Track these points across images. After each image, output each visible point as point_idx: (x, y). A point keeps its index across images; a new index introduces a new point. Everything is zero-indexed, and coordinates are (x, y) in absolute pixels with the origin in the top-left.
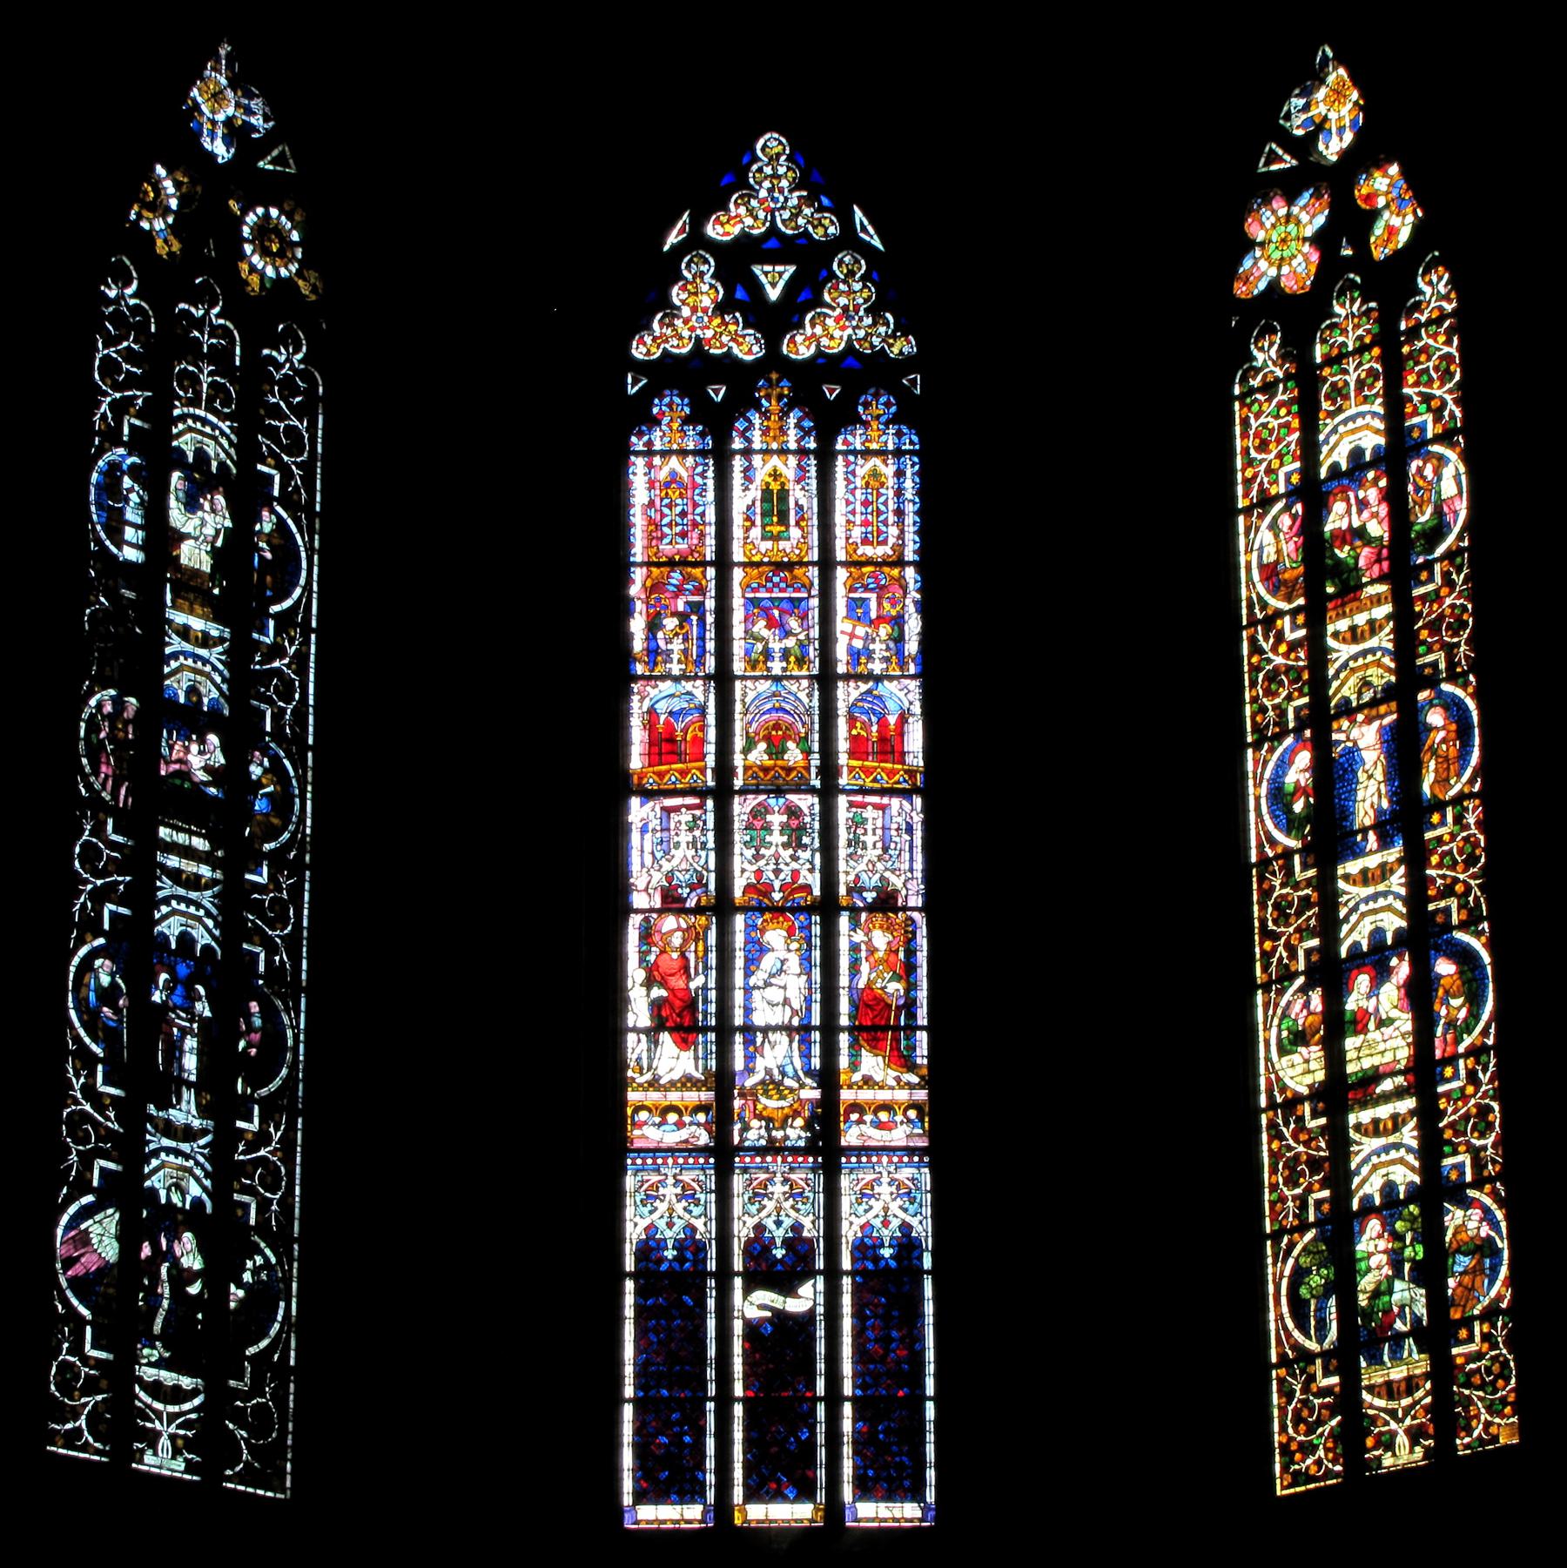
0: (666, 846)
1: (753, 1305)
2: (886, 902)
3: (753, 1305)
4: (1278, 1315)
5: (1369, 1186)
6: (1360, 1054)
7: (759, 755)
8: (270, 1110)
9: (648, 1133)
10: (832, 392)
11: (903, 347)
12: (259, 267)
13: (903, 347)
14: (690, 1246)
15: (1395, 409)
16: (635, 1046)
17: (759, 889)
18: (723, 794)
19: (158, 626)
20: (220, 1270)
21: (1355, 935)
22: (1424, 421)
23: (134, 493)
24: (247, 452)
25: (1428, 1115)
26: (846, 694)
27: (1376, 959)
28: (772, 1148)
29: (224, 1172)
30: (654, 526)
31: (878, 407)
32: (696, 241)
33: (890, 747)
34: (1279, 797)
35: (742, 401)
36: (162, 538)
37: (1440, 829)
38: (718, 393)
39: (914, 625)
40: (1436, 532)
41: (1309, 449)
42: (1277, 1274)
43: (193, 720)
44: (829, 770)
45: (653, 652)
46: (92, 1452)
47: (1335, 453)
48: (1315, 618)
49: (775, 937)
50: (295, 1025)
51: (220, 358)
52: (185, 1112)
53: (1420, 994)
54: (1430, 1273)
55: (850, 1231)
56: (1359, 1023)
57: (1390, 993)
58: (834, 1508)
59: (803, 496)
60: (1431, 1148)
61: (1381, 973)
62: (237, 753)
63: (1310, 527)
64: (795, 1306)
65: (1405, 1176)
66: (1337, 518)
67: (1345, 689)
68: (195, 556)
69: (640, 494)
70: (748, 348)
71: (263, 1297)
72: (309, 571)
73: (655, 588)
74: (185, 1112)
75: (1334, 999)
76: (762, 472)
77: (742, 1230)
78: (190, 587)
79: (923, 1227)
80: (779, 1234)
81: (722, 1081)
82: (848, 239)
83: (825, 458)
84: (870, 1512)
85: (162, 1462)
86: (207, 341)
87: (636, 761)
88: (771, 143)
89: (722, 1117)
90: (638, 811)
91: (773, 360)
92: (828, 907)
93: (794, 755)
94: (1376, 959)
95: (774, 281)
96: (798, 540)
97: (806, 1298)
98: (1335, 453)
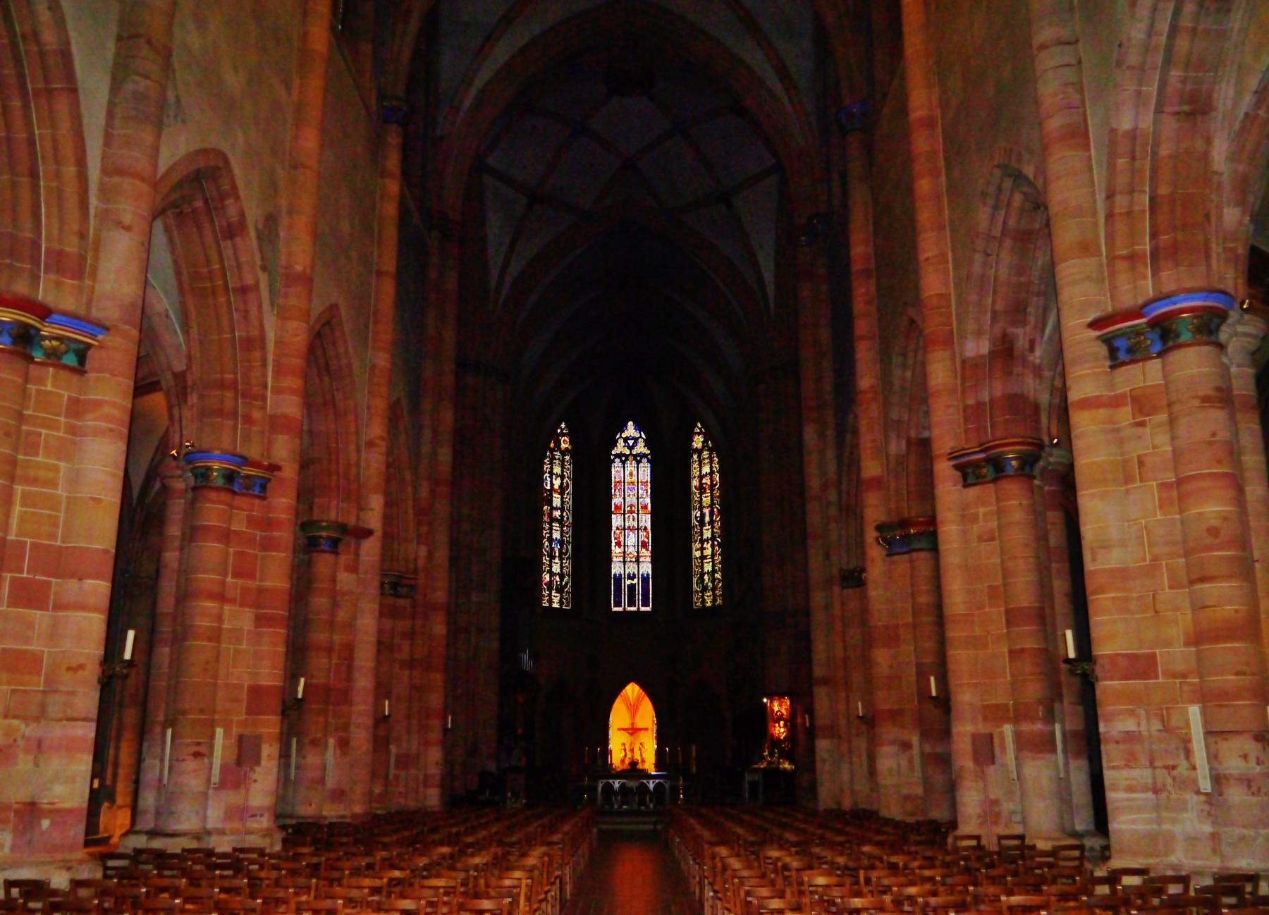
0: (617, 521)
1: (628, 582)
2: (646, 528)
3: (628, 582)
4: (695, 586)
5: (706, 570)
6: (705, 554)
7: (629, 508)
8: (567, 559)
9: (614, 559)
10: (638, 458)
11: (649, 452)
12: (564, 446)
13: (649, 452)
14: (620, 575)
15: (711, 468)
16: (613, 548)
17: (629, 527)
18: (624, 514)
19: (552, 496)
20: (562, 580)
21: (705, 537)
22: (714, 469)
23: (549, 479)
24: (562, 471)
25: (713, 561)
26: (640, 500)
27: (707, 541)
28: (631, 561)
29: (562, 568)
30: (615, 478)
31: (645, 460)
32: (621, 437)
33: (645, 507)
34: (696, 517)
35: (627, 459)
36: (552, 485)
37: (717, 525)
38: (623, 458)
39: (649, 491)
40: (716, 484)
41: (700, 471)
42: (695, 580)
43: (556, 509)
44: (638, 511)
45: (615, 495)
46: (547, 605)
47: (704, 472)
48: (701, 494)
49: (631, 533)
50: (570, 547)
51: (559, 459)
52: (557, 560)
53: (713, 546)
54: (713, 582)
55: (641, 573)
56: (705, 549)
57: (709, 545)
58: (639, 608)
59: (635, 473)
60: (714, 566)
61: (708, 543)
62: (562, 512)
63: (700, 481)
64: (633, 582)
65: (710, 569)
66: (704, 481)
67: (704, 504)
68: (556, 487)
69: (613, 473)
70: (628, 452)
71: (567, 584)
72: (570, 486)
73: (615, 486)
74: (557, 560)
75: (702, 545)
76: (629, 469)
77: (627, 573)
78: (556, 491)
79: (650, 573)
80: (631, 573)
81: (624, 552)
82: (641, 437)
83: (638, 468)
84: (643, 609)
85: (556, 605)
86: (557, 457)
87: (613, 510)
88: (630, 423)
89: (624, 558)
90: (613, 516)
91: (631, 454)
92: (638, 529)
93: (633, 508)
94: (707, 541)
95: (631, 442)
96: (634, 479)
97: (635, 581)
98: (704, 472)
